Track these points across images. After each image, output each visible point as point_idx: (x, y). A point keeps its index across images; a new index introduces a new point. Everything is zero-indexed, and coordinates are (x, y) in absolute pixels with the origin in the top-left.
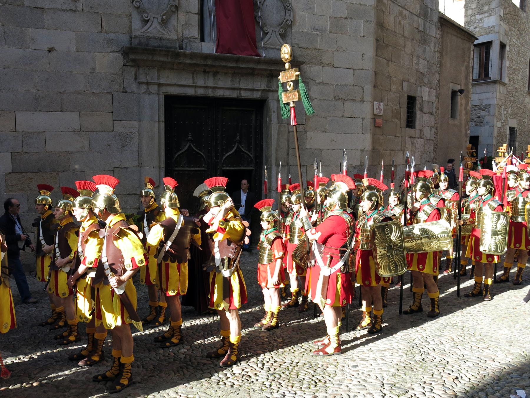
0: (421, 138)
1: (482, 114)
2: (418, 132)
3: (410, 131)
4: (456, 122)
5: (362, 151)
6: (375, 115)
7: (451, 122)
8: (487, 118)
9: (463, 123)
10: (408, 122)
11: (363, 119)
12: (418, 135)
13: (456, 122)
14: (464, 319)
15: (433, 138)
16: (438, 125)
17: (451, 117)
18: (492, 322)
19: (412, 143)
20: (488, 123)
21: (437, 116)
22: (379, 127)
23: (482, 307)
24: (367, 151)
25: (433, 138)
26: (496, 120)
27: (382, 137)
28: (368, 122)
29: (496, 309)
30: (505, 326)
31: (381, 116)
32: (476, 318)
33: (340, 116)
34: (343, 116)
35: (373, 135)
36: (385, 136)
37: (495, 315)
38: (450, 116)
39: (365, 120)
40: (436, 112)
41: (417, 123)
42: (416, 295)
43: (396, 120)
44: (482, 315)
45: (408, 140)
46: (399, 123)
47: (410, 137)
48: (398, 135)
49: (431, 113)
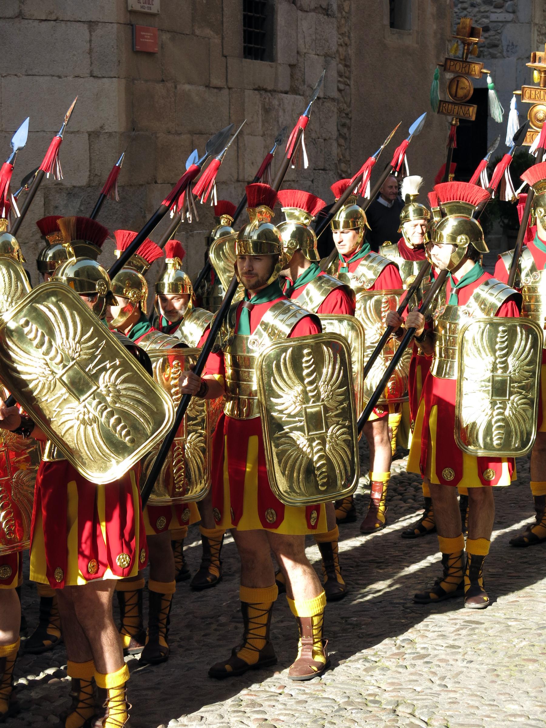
0: (294, 91)
1: (493, 17)
2: (284, 72)
3: (258, 69)
4: (410, 41)
5: (93, 135)
6: (133, 12)
7: (392, 39)
8: (510, 33)
9: (431, 42)
10: (248, 37)
11: (92, 24)
12: (284, 83)
13: (410, 41)
14: (405, 676)
15: (335, 94)
16: (351, 51)
17: (392, 25)
18: (490, 677)
19: (267, 110)
20: (512, 46)
21: (347, 19)
22: (150, 54)
23: (464, 632)
24: (110, 134)
25: (335, 94)
26: (535, 36)
27: (159, 87)
28: (111, 36)
29: (506, 636)
30: (525, 687)
31: (153, 15)
32: (441, 671)
33: (10, 13)
34: (20, 16)
35: (130, 81)
36: (169, 85)
37: (501, 655)
38: (386, 21)
39: (99, 31)
40: (340, 8)
41: (281, 42)
42: (252, 613)
43: (208, 32)
44: (459, 657)
45: (253, 101)
46: (217, 40)
47: (259, 89)
48: (216, 81)
49: (326, 11)
